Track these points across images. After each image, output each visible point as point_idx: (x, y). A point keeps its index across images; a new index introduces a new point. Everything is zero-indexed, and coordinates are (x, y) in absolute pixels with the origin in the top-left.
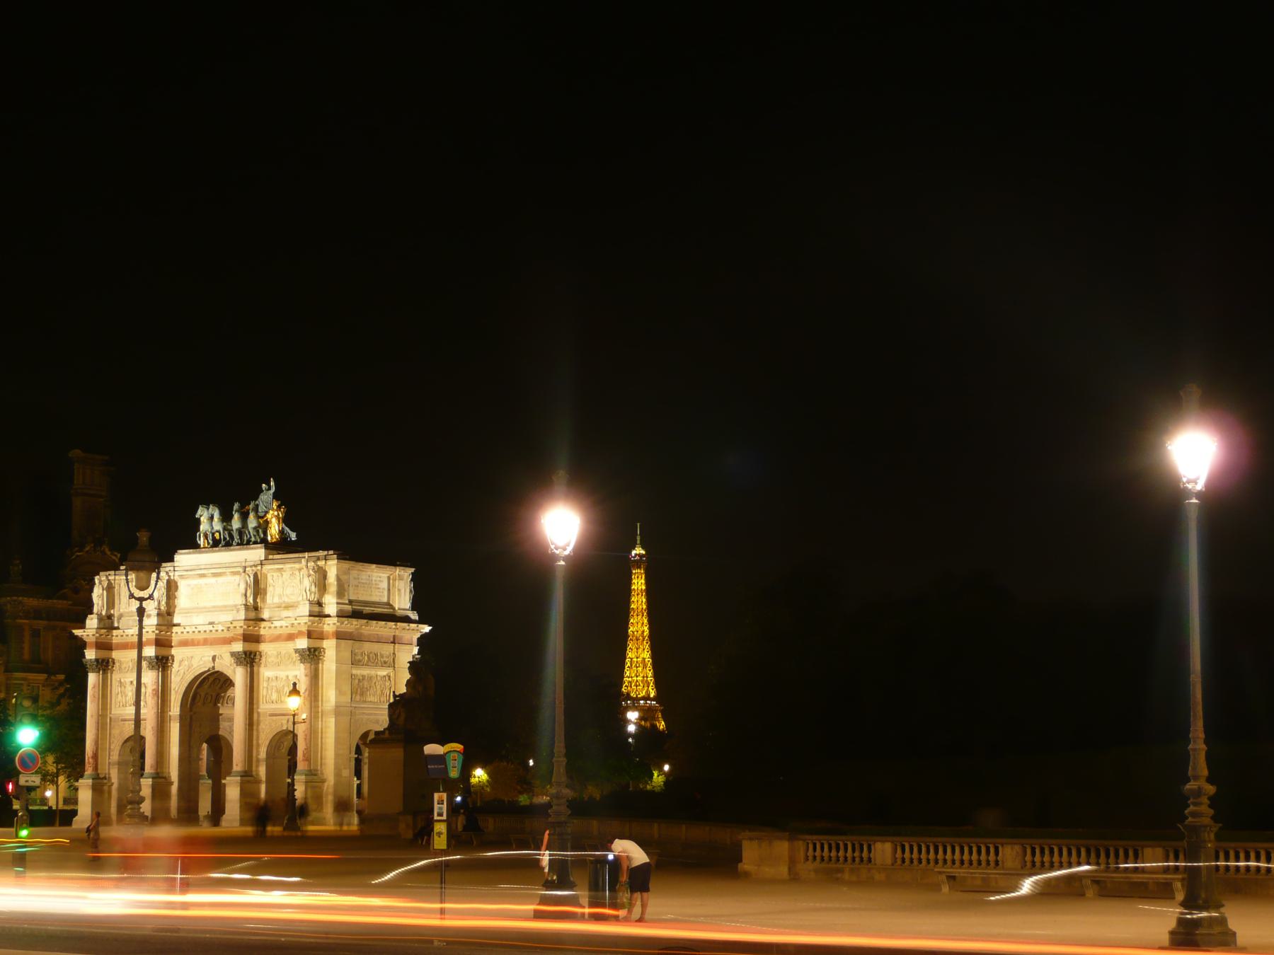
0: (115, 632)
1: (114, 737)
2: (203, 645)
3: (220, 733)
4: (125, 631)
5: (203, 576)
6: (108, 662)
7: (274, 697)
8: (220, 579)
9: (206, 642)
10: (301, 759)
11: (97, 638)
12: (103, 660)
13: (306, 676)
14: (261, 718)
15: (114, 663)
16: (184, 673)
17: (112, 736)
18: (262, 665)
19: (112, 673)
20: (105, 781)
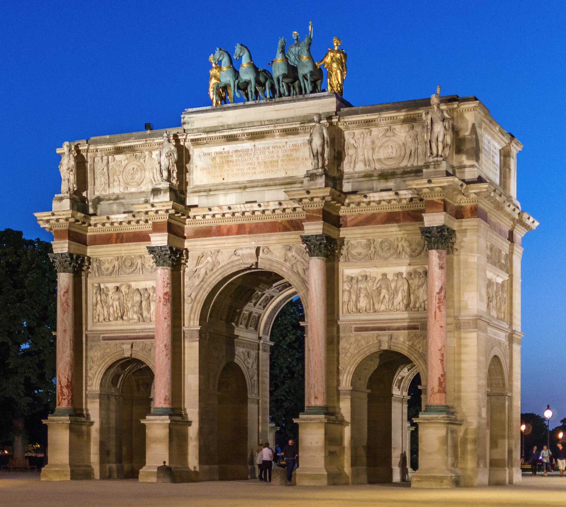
0: (93, 220)
1: (93, 362)
2: (237, 233)
3: (236, 361)
4: (112, 217)
5: (231, 139)
6: (83, 261)
7: (363, 303)
8: (260, 144)
9: (241, 230)
10: (436, 389)
11: (71, 224)
12: (78, 257)
13: (441, 268)
14: (341, 334)
15: (90, 264)
16: (206, 273)
17: (89, 359)
18: (342, 259)
19: (87, 276)
20: (83, 419)
